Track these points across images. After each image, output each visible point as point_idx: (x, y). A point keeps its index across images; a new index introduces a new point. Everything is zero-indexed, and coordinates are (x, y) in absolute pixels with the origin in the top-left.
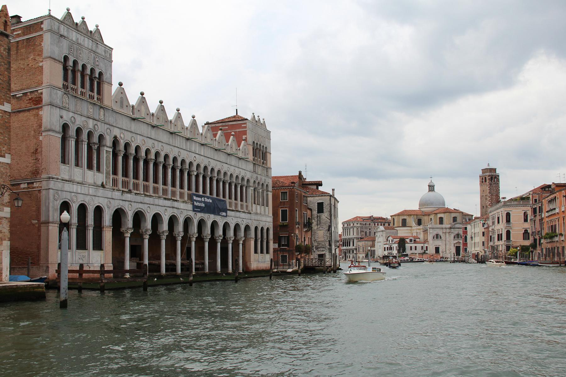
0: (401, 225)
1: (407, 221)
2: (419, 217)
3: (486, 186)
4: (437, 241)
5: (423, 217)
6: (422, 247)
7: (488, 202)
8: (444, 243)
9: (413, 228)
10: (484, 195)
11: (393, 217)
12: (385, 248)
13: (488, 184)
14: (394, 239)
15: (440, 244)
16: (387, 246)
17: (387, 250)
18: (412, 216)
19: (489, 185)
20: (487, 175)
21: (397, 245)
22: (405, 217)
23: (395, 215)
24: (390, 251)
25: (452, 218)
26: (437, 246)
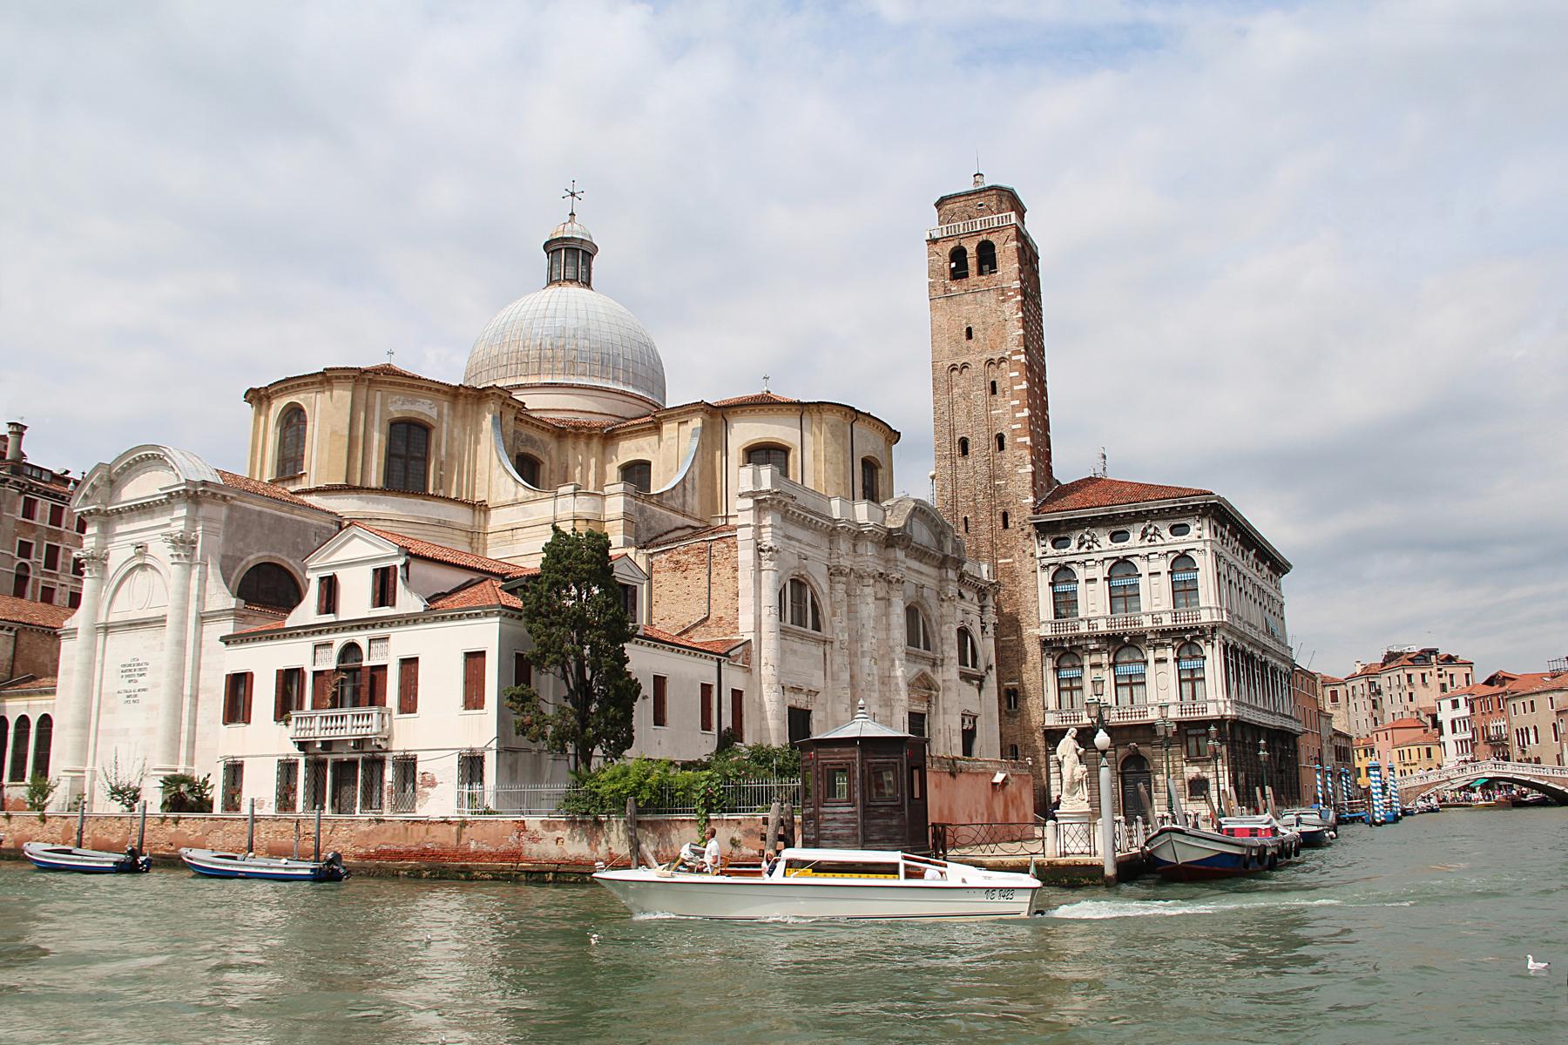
0: (375, 478)
2: (530, 441)
3: (990, 299)
4: (797, 645)
5: (553, 445)
6: (706, 689)
8: (846, 676)
9: (497, 520)
10: (976, 360)
11: (278, 405)
12: (239, 685)
13: (1017, 284)
14: (416, 567)
15: (817, 681)
17: (285, 706)
21: (486, 634)
22: (424, 408)
23: (325, 379)
24: (350, 725)
26: (801, 701)
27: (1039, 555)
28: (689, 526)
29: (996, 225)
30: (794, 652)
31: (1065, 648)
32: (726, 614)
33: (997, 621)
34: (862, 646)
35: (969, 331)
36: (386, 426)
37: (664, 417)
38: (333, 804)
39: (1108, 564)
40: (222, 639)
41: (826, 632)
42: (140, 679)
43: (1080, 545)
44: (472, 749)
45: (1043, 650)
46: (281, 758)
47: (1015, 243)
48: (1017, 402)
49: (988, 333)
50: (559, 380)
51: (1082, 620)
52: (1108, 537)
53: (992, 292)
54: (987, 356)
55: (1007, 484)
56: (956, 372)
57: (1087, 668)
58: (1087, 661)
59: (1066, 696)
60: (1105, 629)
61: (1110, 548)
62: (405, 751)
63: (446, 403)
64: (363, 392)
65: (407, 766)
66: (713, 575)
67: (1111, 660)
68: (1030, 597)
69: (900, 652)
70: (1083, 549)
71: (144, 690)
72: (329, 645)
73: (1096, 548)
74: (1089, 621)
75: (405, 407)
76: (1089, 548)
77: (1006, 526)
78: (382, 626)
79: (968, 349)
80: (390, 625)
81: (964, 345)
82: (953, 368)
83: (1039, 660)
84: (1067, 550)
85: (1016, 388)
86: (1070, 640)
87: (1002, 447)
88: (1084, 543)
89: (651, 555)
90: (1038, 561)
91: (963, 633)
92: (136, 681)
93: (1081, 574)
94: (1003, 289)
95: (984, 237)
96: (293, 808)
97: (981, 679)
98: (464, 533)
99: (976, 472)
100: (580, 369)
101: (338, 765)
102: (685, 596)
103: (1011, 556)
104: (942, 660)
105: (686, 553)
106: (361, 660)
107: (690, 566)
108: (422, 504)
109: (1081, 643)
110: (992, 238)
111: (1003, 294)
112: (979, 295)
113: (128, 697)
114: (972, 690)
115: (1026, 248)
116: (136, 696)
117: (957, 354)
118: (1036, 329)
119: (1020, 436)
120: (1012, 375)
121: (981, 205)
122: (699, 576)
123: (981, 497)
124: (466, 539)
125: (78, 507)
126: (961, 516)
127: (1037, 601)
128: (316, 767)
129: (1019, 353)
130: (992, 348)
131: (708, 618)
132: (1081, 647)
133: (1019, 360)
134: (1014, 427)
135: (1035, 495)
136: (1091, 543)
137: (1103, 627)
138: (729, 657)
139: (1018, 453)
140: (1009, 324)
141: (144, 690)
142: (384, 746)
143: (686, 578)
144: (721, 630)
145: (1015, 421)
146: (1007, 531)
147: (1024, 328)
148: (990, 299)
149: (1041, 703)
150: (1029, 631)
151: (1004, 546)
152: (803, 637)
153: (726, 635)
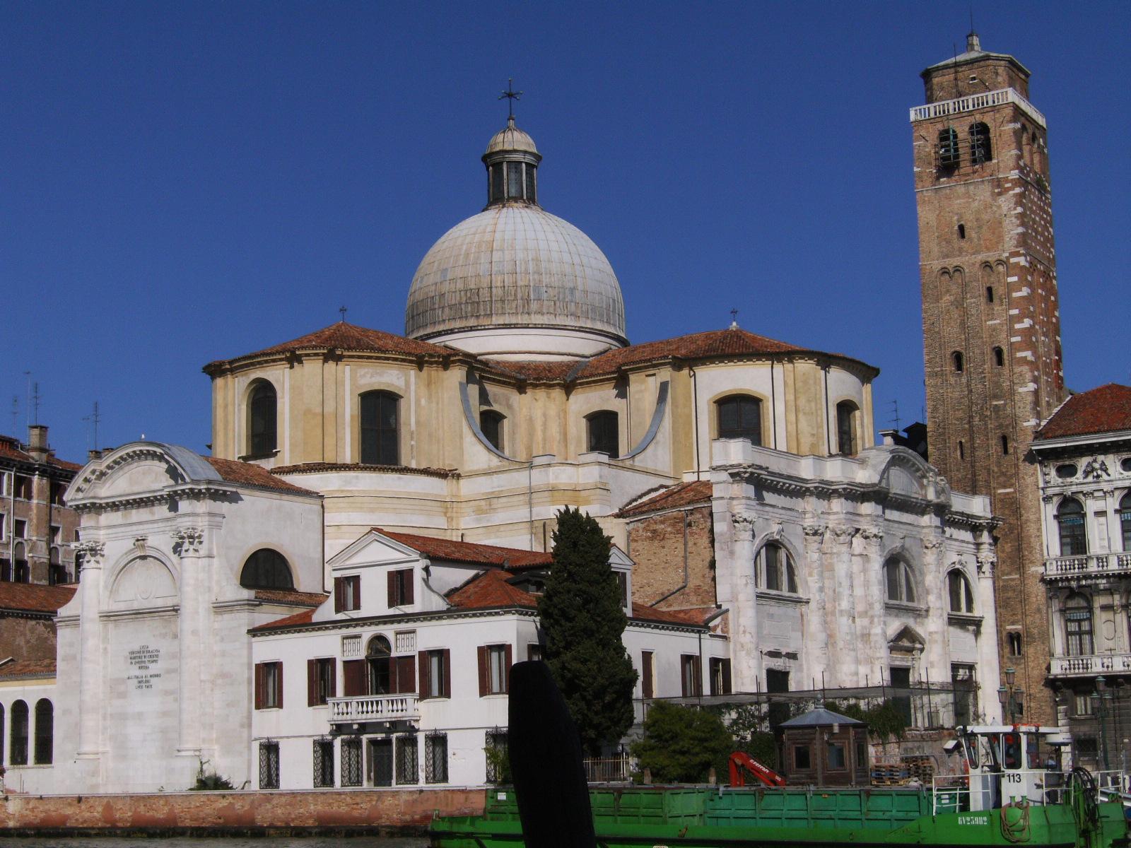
0: (349, 451)
1: (410, 416)
3: (983, 192)
4: (774, 608)
6: (686, 659)
7: (1019, 319)
9: (467, 488)
10: (970, 261)
13: (1014, 174)
16: (328, 645)
18: (457, 374)
19: (1018, 182)
20: (995, 109)
24: (385, 709)
25: (833, 412)
26: (778, 664)
27: (1041, 485)
28: (662, 486)
29: (991, 103)
30: (771, 616)
31: (1071, 589)
32: (703, 582)
33: (995, 560)
34: (839, 604)
35: (961, 228)
36: (357, 400)
37: (631, 370)
38: (369, 778)
39: (1118, 495)
40: (249, 632)
41: (801, 594)
42: (151, 666)
43: (1087, 474)
44: (497, 727)
45: (1048, 590)
46: (316, 738)
47: (1012, 126)
48: (1015, 312)
49: (983, 230)
50: (514, 321)
51: (1091, 558)
52: (1119, 464)
53: (986, 183)
54: (981, 257)
55: (1005, 405)
56: (947, 276)
57: (1097, 612)
58: (1099, 601)
59: (1074, 640)
60: (1117, 567)
61: (1121, 476)
62: (436, 730)
63: (412, 372)
64: (331, 365)
65: (438, 741)
66: (690, 544)
67: (1124, 601)
68: (1031, 529)
69: (878, 608)
70: (1090, 479)
71: (157, 676)
72: (358, 637)
73: (1105, 477)
74: (1098, 559)
75: (374, 380)
76: (1098, 476)
77: (1006, 452)
78: (407, 622)
79: (961, 250)
80: (418, 620)
81: (956, 246)
82: (944, 271)
83: (1043, 601)
84: (1073, 479)
85: (1015, 295)
86: (1078, 579)
87: (1000, 362)
88: (1092, 471)
89: (628, 524)
90: (1041, 492)
91: (956, 575)
92: (147, 668)
93: (1091, 506)
94: (999, 180)
95: (978, 118)
96: (332, 783)
97: (977, 623)
98: (439, 504)
99: (971, 391)
100: (534, 306)
101: (372, 742)
102: (663, 565)
103: (1011, 486)
104: (927, 611)
105: (662, 522)
106: (389, 648)
107: (667, 536)
108: (399, 478)
109: (1089, 582)
110: (987, 120)
111: (999, 186)
112: (971, 188)
113: (140, 682)
114: (965, 637)
115: (1028, 125)
116: (147, 681)
117: (947, 256)
118: (1042, 218)
119: (1019, 351)
120: (1010, 280)
121: (974, 79)
122: (676, 545)
123: (977, 419)
124: (441, 509)
125: (72, 500)
126: (954, 441)
127: (1039, 536)
128: (353, 745)
129: (1017, 254)
130: (986, 247)
131: (685, 587)
132: (1090, 586)
133: (1017, 263)
134: (1014, 339)
135: (1039, 416)
136: (1099, 472)
137: (1113, 566)
138: (709, 628)
139: (1017, 369)
140: (1006, 222)
141: (157, 676)
142: (417, 727)
143: (663, 547)
144: (700, 598)
145: (1012, 332)
146: (1007, 458)
147: (1023, 224)
148: (983, 192)
149: (1047, 649)
150: (1033, 569)
151: (1003, 474)
152: (780, 599)
153: (704, 603)
